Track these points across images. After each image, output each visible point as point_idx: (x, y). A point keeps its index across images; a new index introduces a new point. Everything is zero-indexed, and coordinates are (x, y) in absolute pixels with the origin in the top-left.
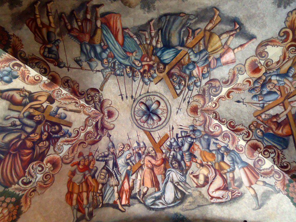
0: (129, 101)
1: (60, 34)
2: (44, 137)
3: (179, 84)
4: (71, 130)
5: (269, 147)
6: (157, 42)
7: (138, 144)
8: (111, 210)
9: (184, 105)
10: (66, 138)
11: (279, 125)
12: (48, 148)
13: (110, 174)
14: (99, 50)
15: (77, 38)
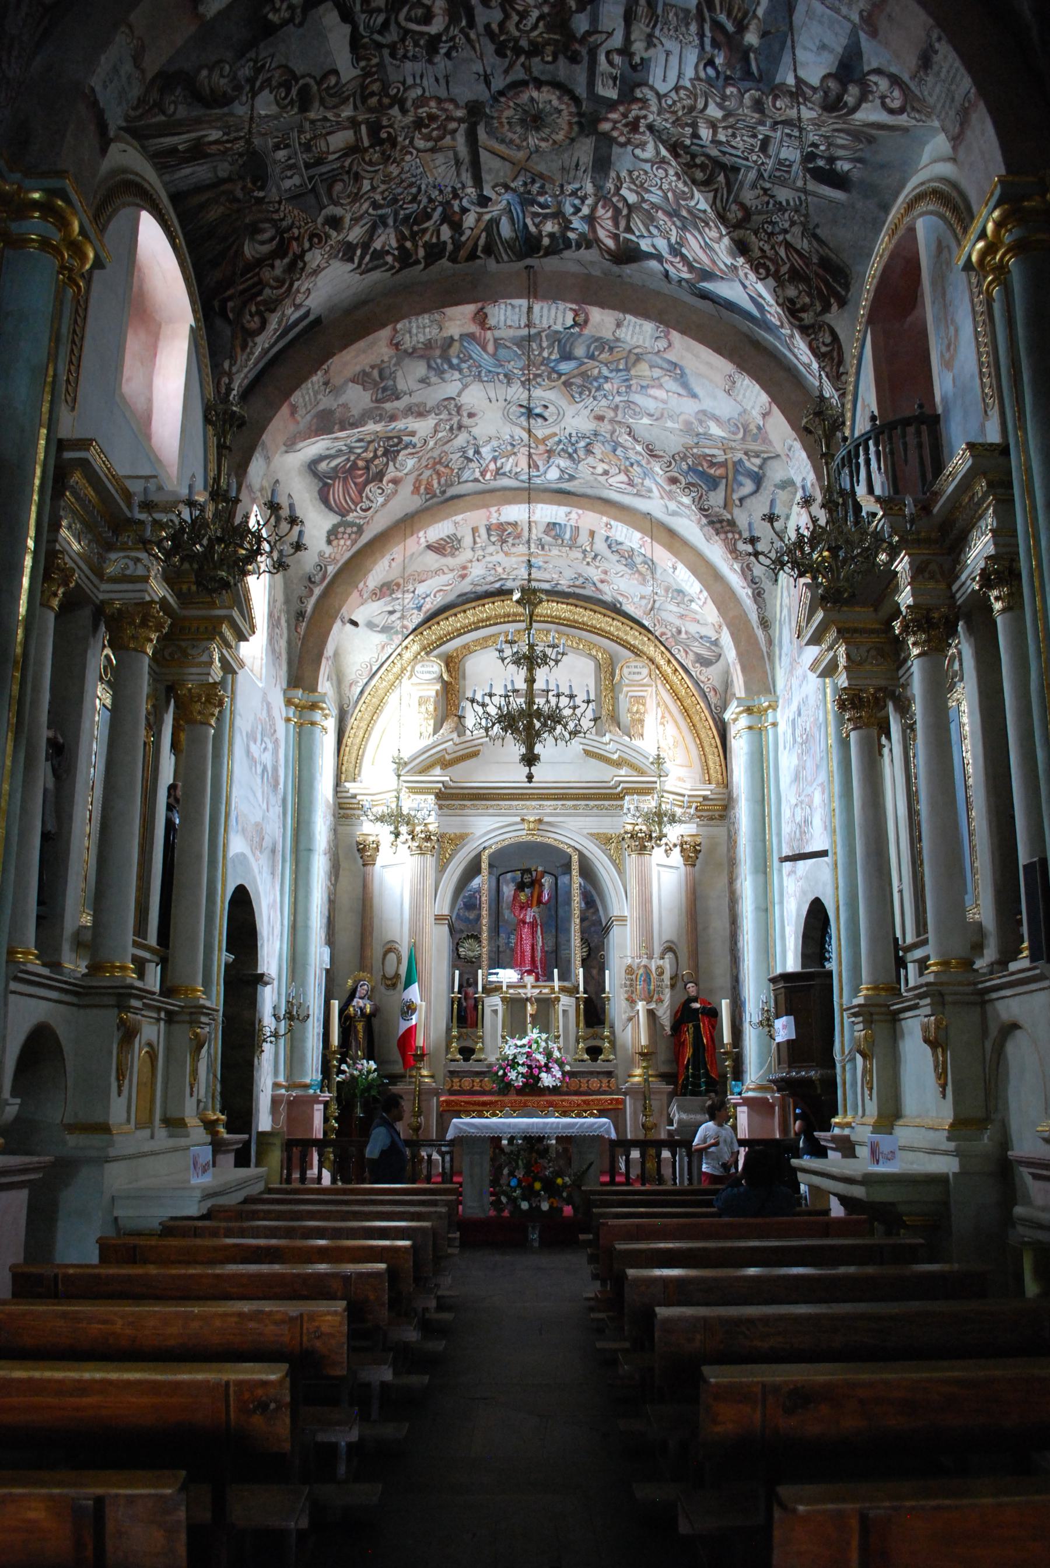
1: (397, 364)
2: (379, 453)
3: (581, 394)
4: (414, 440)
5: (693, 485)
6: (550, 354)
7: (512, 437)
8: (470, 484)
9: (587, 412)
10: (409, 451)
11: (712, 464)
12: (387, 464)
13: (470, 460)
14: (455, 361)
15: (421, 357)
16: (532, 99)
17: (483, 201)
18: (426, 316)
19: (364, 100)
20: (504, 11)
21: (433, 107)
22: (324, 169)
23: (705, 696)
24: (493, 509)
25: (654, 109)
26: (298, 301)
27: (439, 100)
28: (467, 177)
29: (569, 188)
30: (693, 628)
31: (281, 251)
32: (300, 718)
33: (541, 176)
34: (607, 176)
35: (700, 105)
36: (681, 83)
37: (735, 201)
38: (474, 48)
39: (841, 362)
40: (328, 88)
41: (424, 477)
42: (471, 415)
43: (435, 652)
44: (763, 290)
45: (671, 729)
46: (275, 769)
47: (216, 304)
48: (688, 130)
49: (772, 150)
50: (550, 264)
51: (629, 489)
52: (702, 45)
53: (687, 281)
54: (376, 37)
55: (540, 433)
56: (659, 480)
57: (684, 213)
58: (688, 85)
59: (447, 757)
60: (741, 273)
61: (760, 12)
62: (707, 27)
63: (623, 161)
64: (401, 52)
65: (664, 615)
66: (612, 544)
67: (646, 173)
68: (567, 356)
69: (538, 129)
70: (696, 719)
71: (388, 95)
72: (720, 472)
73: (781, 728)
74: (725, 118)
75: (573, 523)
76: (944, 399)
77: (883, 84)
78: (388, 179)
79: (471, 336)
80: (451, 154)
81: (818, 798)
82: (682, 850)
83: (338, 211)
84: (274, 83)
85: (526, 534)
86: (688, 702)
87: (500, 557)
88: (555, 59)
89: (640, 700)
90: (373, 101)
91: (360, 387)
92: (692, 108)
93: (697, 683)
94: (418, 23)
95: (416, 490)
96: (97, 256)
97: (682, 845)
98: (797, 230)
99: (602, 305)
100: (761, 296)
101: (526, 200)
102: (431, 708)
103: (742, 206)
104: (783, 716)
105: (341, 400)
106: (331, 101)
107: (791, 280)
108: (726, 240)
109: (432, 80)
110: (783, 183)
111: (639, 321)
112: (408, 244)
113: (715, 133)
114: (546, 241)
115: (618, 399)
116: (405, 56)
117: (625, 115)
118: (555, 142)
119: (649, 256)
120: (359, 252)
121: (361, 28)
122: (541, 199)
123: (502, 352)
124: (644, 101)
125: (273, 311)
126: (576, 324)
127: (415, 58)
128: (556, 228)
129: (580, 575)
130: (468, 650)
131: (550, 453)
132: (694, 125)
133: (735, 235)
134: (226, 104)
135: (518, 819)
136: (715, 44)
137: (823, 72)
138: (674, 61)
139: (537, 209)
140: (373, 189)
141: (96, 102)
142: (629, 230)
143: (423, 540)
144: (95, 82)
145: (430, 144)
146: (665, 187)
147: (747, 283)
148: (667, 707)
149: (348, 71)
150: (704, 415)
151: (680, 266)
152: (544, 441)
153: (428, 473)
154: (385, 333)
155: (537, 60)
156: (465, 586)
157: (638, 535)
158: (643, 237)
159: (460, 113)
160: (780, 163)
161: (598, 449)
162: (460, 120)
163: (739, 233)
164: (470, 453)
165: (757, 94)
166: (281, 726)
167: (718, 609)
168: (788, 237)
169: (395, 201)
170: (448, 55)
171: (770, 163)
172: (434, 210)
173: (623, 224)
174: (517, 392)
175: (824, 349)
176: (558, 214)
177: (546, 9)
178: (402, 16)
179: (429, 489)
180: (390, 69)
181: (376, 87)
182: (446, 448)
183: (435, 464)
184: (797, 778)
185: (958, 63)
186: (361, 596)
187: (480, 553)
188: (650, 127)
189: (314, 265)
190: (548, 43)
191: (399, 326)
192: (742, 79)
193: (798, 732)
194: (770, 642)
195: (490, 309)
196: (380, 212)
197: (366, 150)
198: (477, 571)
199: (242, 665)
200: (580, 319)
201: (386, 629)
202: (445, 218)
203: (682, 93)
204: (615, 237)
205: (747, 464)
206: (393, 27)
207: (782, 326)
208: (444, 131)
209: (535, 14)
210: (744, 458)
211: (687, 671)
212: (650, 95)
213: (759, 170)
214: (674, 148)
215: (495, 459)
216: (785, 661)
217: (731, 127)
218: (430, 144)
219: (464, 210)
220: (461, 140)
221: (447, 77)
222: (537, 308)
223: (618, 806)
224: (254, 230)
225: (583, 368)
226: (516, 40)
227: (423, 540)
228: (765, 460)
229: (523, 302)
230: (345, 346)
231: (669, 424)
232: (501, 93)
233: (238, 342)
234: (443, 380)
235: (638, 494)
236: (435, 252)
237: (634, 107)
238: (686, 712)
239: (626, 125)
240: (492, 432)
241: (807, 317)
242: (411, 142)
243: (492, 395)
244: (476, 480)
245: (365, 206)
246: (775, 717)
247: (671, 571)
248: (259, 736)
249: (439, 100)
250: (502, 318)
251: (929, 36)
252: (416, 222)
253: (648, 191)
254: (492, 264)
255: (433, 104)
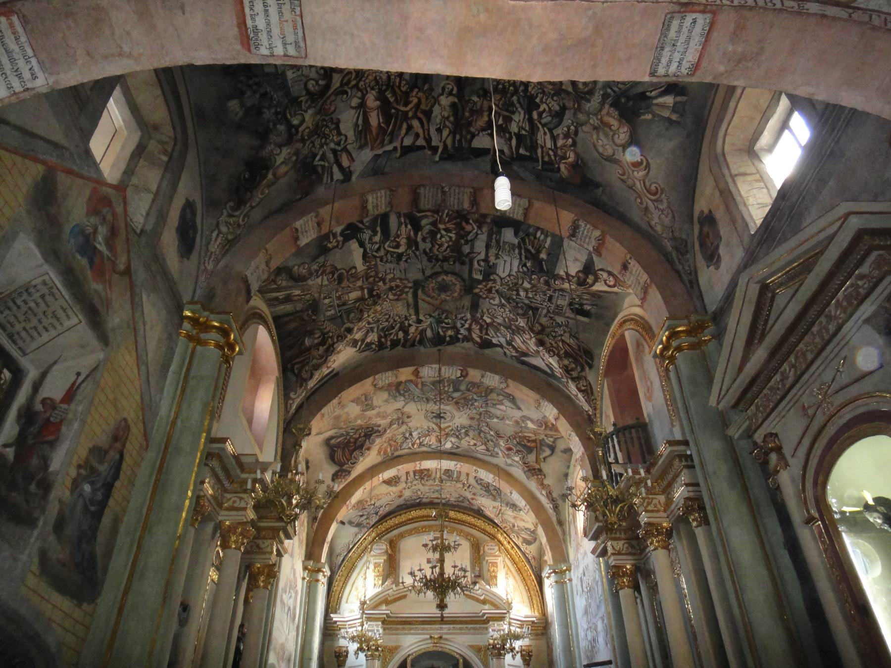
0: (424, 412)
1: (374, 393)
2: (363, 434)
3: (463, 407)
4: (380, 429)
7: (428, 427)
9: (465, 416)
11: (529, 441)
12: (365, 441)
13: (407, 438)
14: (402, 392)
15: (385, 390)
16: (443, 279)
17: (419, 321)
18: (390, 372)
19: (367, 279)
20: (432, 244)
21: (398, 282)
22: (345, 307)
23: (529, 561)
24: (418, 463)
25: (499, 283)
26: (329, 365)
27: (401, 279)
28: (412, 311)
29: (459, 316)
30: (522, 524)
31: (322, 343)
32: (310, 577)
33: (447, 311)
34: (477, 312)
35: (520, 282)
36: (511, 273)
37: (537, 322)
38: (418, 259)
39: (592, 393)
40: (351, 274)
41: (383, 447)
42: (409, 417)
43: (384, 538)
44: (553, 362)
45: (511, 581)
46: (295, 608)
47: (289, 366)
48: (515, 293)
49: (554, 301)
50: (450, 349)
51: (487, 453)
52: (521, 258)
53: (515, 356)
54: (374, 253)
55: (442, 426)
56: (502, 448)
57: (513, 327)
58: (515, 274)
59: (389, 599)
60: (541, 354)
61: (547, 246)
62: (523, 251)
63: (485, 305)
64: (385, 259)
65: (505, 517)
66: (479, 481)
67: (495, 310)
68: (456, 390)
69: (445, 292)
70: (525, 575)
71: (378, 277)
72: (533, 445)
73: (575, 582)
74: (531, 288)
75: (458, 469)
76: (648, 415)
77: (605, 275)
78: (375, 312)
79: (411, 381)
80: (405, 302)
81: (600, 626)
82: (522, 656)
83: (351, 325)
84: (327, 272)
85: (434, 475)
86: (520, 565)
87: (420, 487)
88: (454, 263)
89: (495, 564)
90: (371, 280)
91: (355, 404)
92: (516, 284)
93: (524, 554)
94: (393, 248)
95: (379, 453)
96: (240, 349)
97: (521, 652)
98: (567, 335)
99: (474, 367)
100: (551, 364)
101: (439, 321)
102: (381, 569)
103: (541, 324)
104: (575, 575)
105: (346, 410)
106: (352, 280)
107: (565, 357)
108: (534, 339)
109: (398, 272)
110: (559, 314)
111: (493, 375)
112: (383, 340)
113: (527, 294)
114: (448, 339)
115: (481, 410)
116: (387, 261)
117: (486, 286)
118: (453, 297)
119: (496, 346)
120: (359, 343)
121: (368, 250)
122: (446, 321)
123: (426, 388)
124: (494, 281)
125: (316, 370)
126: (462, 376)
127: (391, 262)
128: (453, 333)
129: (461, 496)
130: (401, 536)
131: (447, 435)
132: (517, 291)
133: (537, 337)
134: (305, 281)
135: (428, 636)
136: (526, 258)
137: (577, 270)
138: (508, 265)
139: (444, 325)
140: (369, 316)
141: (247, 281)
142: (487, 334)
143: (381, 478)
144: (248, 273)
145: (396, 297)
146: (504, 316)
147: (545, 358)
148: (509, 568)
149: (360, 266)
150: (525, 418)
151: (512, 350)
152: (444, 429)
153: (385, 445)
154: (370, 380)
155: (446, 264)
156: (401, 501)
157: (491, 476)
158: (493, 337)
159: (410, 285)
160: (558, 306)
161: (471, 433)
162: (410, 288)
163: (540, 336)
164: (407, 435)
165: (547, 278)
166: (299, 581)
167: (535, 515)
168: (563, 338)
169: (378, 321)
170: (406, 261)
171: (553, 307)
172: (396, 325)
173: (484, 332)
174: (433, 407)
175: (583, 388)
176: (454, 327)
177: (451, 243)
178: (386, 246)
179: (385, 453)
180: (380, 267)
181: (373, 274)
182: (395, 432)
183: (389, 440)
184: (586, 612)
185: (640, 268)
186: (347, 508)
187: (410, 484)
188: (497, 291)
189: (338, 350)
190: (451, 257)
191: (376, 377)
192: (539, 272)
193: (584, 585)
194: (564, 533)
195: (420, 369)
196: (371, 326)
197: (366, 299)
198: (407, 494)
199: (286, 552)
200: (464, 374)
201: (358, 525)
202: (400, 329)
203: (512, 278)
204: (481, 337)
205: (547, 441)
206: (382, 249)
207: (562, 377)
208: (402, 292)
209: (446, 245)
210: (545, 438)
211: (519, 548)
212: (497, 278)
213: (548, 310)
214: (508, 299)
215: (419, 438)
216: (573, 544)
217: (535, 291)
218: (396, 297)
219: (410, 325)
220: (410, 295)
221: (405, 270)
222: (443, 369)
223: (484, 628)
224: (311, 333)
225: (465, 395)
226: (437, 256)
227: (381, 478)
228: (556, 439)
229: (437, 366)
230: (350, 386)
231: (507, 422)
232: (430, 277)
233: (298, 384)
234: (396, 401)
235: (492, 455)
236: (395, 343)
237: (490, 283)
238: (519, 571)
239: (486, 290)
240: (419, 425)
241: (575, 374)
242: (387, 297)
243: (419, 408)
244: (410, 448)
245: (364, 323)
246: (570, 576)
247: (509, 494)
248: (288, 589)
249: (401, 279)
250: (426, 373)
251: (625, 257)
252: (387, 330)
253: (496, 318)
254: (422, 349)
255: (398, 281)
